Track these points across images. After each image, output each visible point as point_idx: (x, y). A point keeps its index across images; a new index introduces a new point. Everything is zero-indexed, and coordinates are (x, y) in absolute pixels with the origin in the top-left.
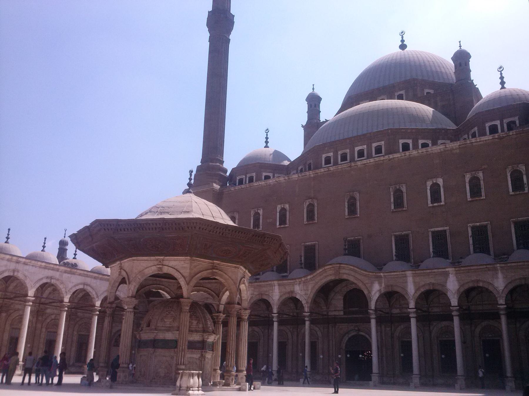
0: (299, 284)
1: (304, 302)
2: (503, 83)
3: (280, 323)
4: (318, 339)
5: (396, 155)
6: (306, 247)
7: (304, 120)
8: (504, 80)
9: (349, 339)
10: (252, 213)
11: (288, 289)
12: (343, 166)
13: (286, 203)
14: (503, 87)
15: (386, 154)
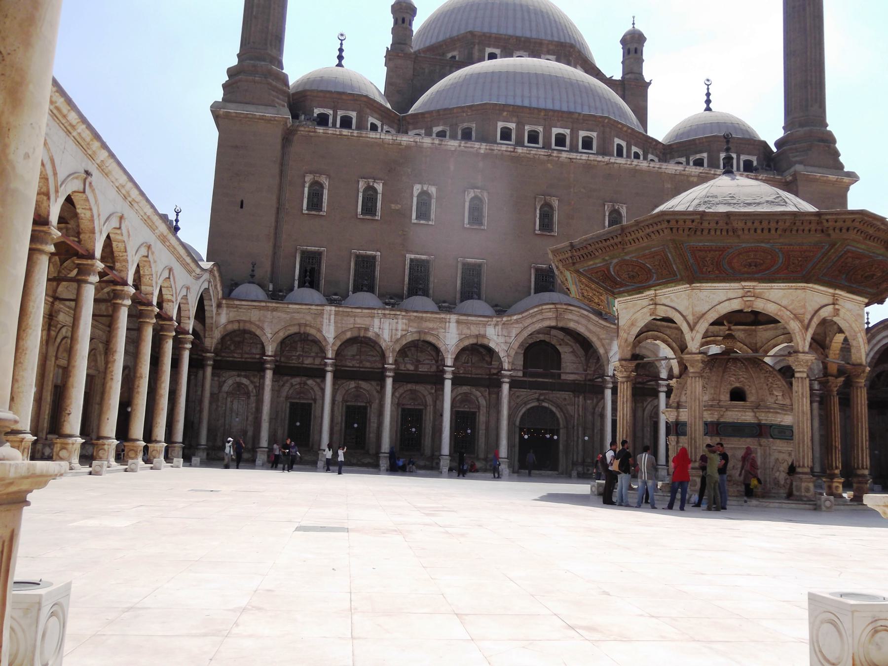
0: (496, 325)
1: (502, 354)
2: (708, 102)
3: (456, 382)
4: (479, 408)
5: (606, 159)
6: (464, 264)
7: (387, 40)
8: (711, 98)
9: (528, 410)
10: (362, 185)
11: (474, 330)
12: (537, 151)
13: (434, 185)
14: (708, 109)
15: (597, 154)
